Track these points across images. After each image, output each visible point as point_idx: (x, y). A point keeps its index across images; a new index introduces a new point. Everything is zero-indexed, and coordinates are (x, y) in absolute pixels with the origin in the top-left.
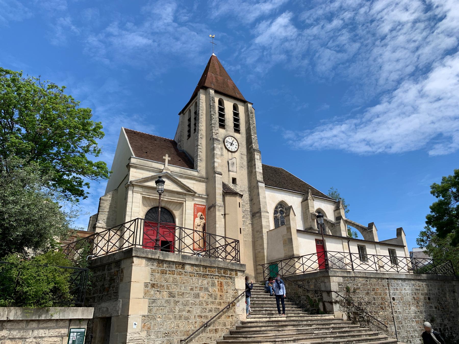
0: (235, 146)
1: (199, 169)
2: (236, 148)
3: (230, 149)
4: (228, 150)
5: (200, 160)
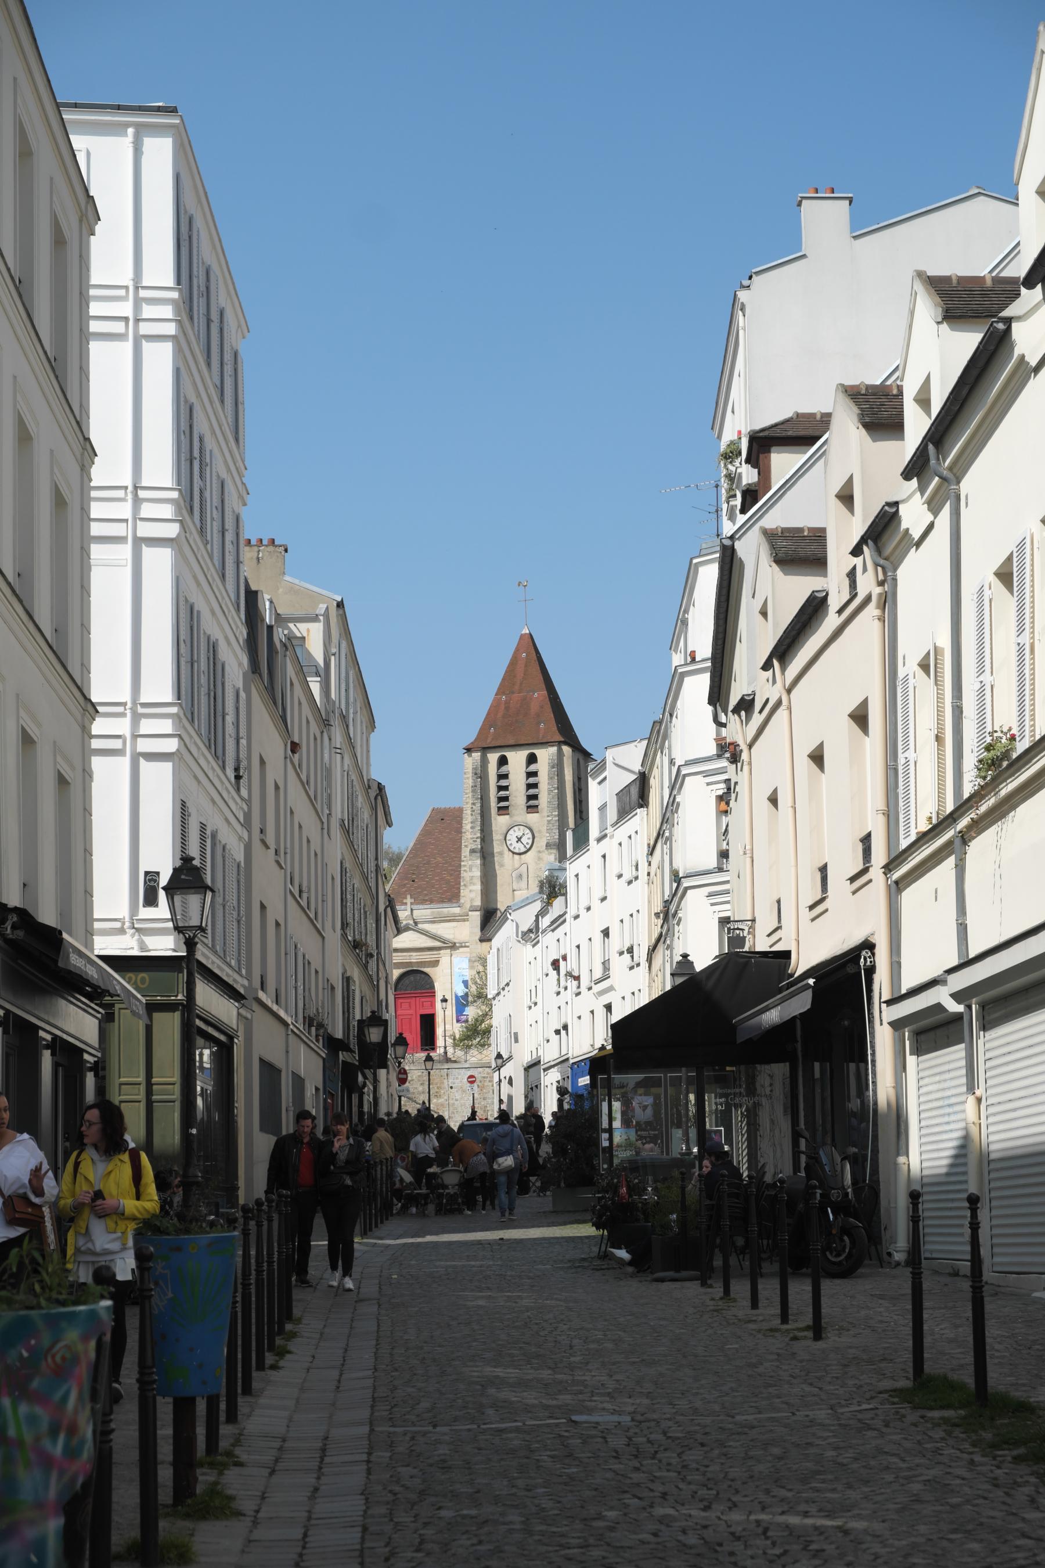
0: (515, 844)
1: (462, 901)
2: (527, 843)
3: (516, 851)
4: (514, 853)
5: (465, 885)
